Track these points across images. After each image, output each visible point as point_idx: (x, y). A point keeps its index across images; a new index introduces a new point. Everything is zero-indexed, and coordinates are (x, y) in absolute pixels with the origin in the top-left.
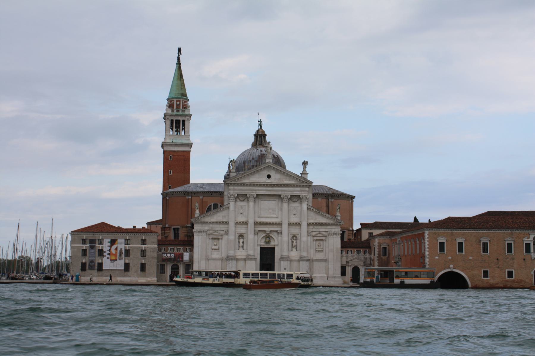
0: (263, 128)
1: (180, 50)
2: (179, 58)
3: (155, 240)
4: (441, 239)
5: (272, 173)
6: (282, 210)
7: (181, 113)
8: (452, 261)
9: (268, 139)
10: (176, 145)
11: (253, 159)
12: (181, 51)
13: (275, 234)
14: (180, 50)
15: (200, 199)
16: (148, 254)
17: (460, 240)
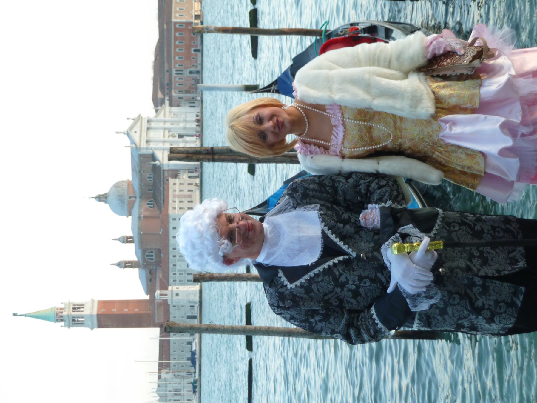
0: (95, 196)
1: (15, 315)
2: (21, 315)
3: (174, 180)
4: (177, 15)
5: (134, 130)
6: (156, 129)
7: (67, 307)
8: (188, 12)
9: (102, 193)
10: (93, 307)
11: (117, 190)
12: (15, 313)
13: (170, 133)
14: (15, 315)
15: (144, 211)
16: (182, 182)
17: (178, 9)
